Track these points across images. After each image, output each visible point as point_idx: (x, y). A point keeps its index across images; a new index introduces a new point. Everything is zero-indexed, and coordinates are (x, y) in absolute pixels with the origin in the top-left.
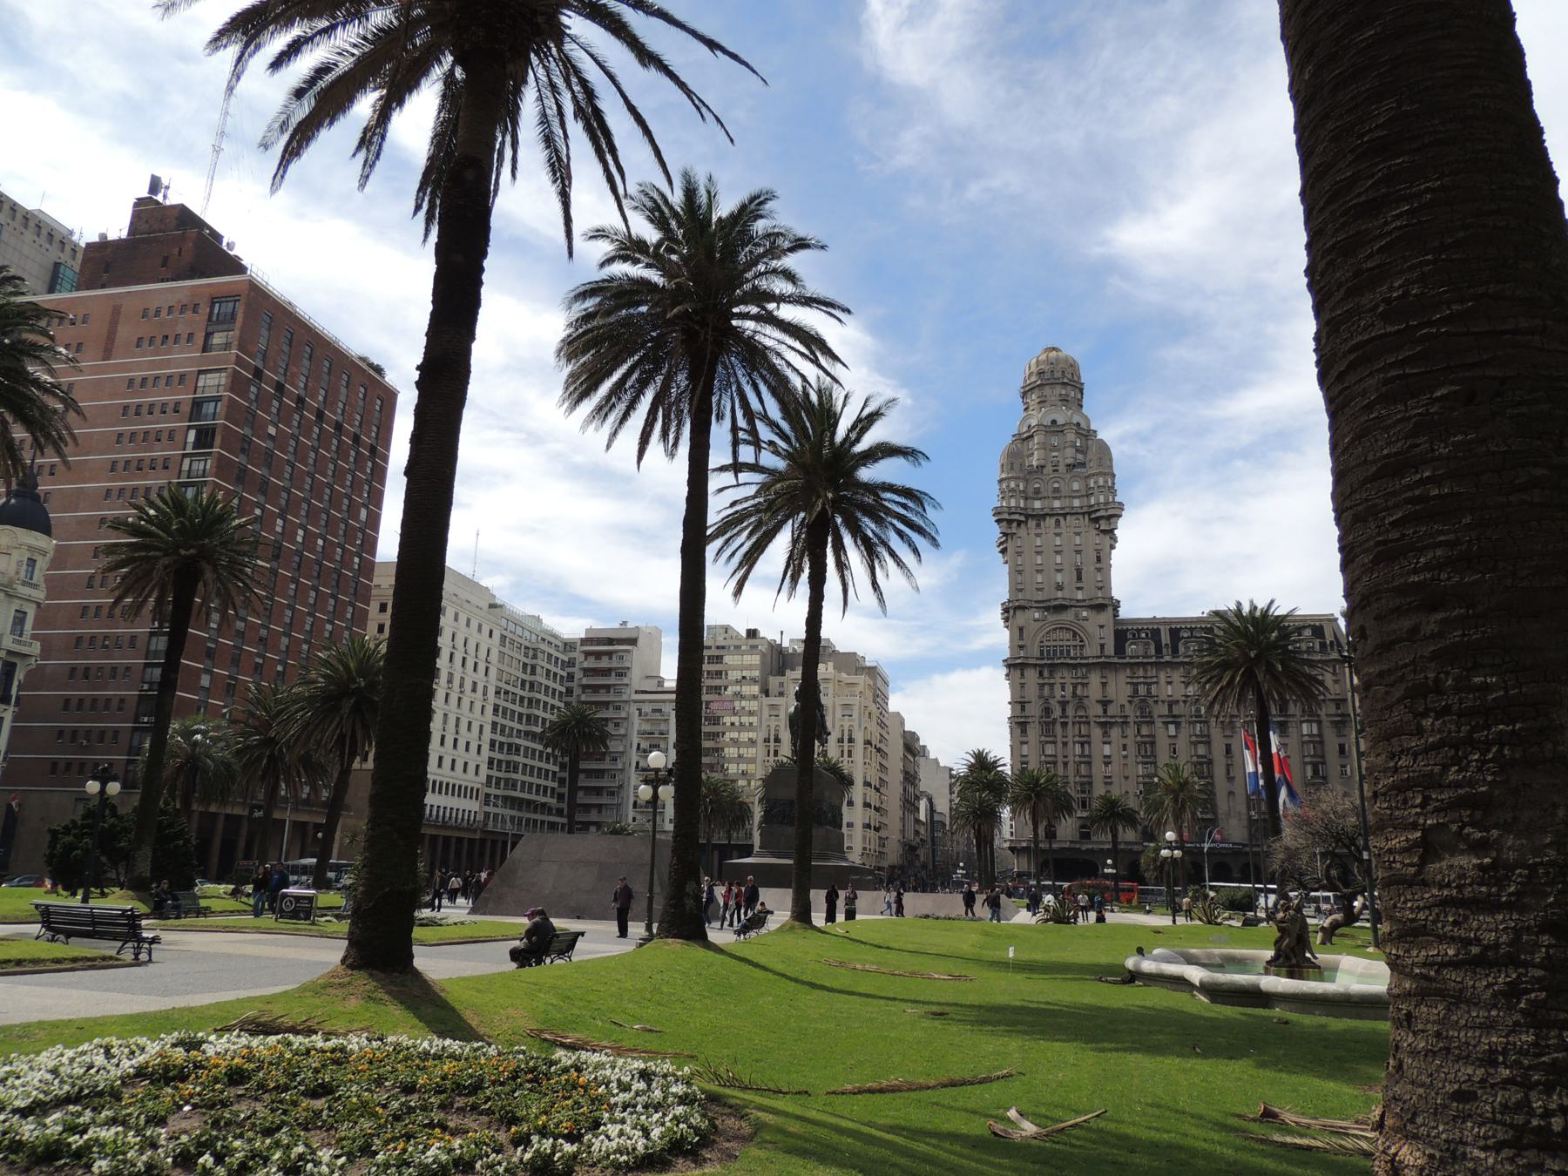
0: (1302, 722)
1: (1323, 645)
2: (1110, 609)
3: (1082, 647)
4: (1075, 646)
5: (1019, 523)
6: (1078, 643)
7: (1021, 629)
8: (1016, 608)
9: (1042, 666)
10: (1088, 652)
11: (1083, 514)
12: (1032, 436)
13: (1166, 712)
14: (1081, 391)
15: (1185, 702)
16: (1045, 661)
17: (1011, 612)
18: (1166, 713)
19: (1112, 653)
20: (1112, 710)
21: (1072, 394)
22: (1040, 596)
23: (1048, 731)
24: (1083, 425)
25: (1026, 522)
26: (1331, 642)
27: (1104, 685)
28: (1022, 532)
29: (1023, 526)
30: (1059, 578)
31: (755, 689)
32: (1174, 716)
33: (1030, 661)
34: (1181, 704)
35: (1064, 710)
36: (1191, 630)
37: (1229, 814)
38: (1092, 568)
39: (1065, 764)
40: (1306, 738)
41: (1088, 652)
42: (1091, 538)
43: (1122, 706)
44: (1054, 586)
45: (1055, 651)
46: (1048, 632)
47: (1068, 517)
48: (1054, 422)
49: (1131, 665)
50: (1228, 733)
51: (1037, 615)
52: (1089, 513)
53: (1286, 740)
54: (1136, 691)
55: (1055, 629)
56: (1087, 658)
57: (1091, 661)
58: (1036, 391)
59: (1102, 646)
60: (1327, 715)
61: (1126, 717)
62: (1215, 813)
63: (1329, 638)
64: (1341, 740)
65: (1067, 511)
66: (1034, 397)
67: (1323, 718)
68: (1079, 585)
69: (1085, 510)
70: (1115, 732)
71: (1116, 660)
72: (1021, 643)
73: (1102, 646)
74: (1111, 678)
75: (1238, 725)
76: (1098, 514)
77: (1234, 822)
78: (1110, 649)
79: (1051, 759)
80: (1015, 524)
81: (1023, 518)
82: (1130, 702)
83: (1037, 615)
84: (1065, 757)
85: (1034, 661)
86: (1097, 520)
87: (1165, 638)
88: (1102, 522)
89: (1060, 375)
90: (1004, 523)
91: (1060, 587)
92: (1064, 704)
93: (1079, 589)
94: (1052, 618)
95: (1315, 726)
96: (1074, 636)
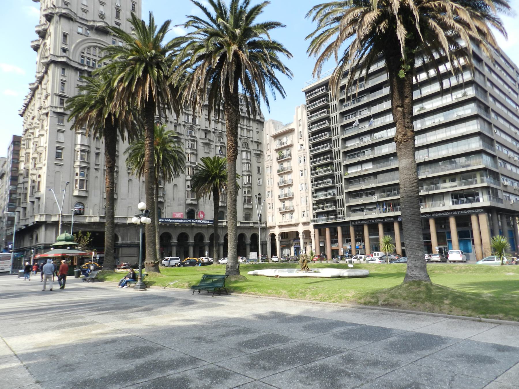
0: (242, 151)
7: (65, 36)
8: (62, 16)
9: (82, 72)
15: (184, 126)
16: (86, 68)
17: (56, 18)
22: (84, 16)
30: (101, 9)
32: (178, 133)
33: (73, 64)
34: (182, 126)
39: (97, 155)
40: (245, 161)
46: (89, 48)
50: (207, 151)
51: (80, 30)
55: (95, 47)
60: (254, 150)
64: (259, 165)
67: (252, 151)
75: (212, 147)
79: (86, 148)
83: (80, 30)
85: (76, 65)
94: (93, 36)
95: (249, 154)
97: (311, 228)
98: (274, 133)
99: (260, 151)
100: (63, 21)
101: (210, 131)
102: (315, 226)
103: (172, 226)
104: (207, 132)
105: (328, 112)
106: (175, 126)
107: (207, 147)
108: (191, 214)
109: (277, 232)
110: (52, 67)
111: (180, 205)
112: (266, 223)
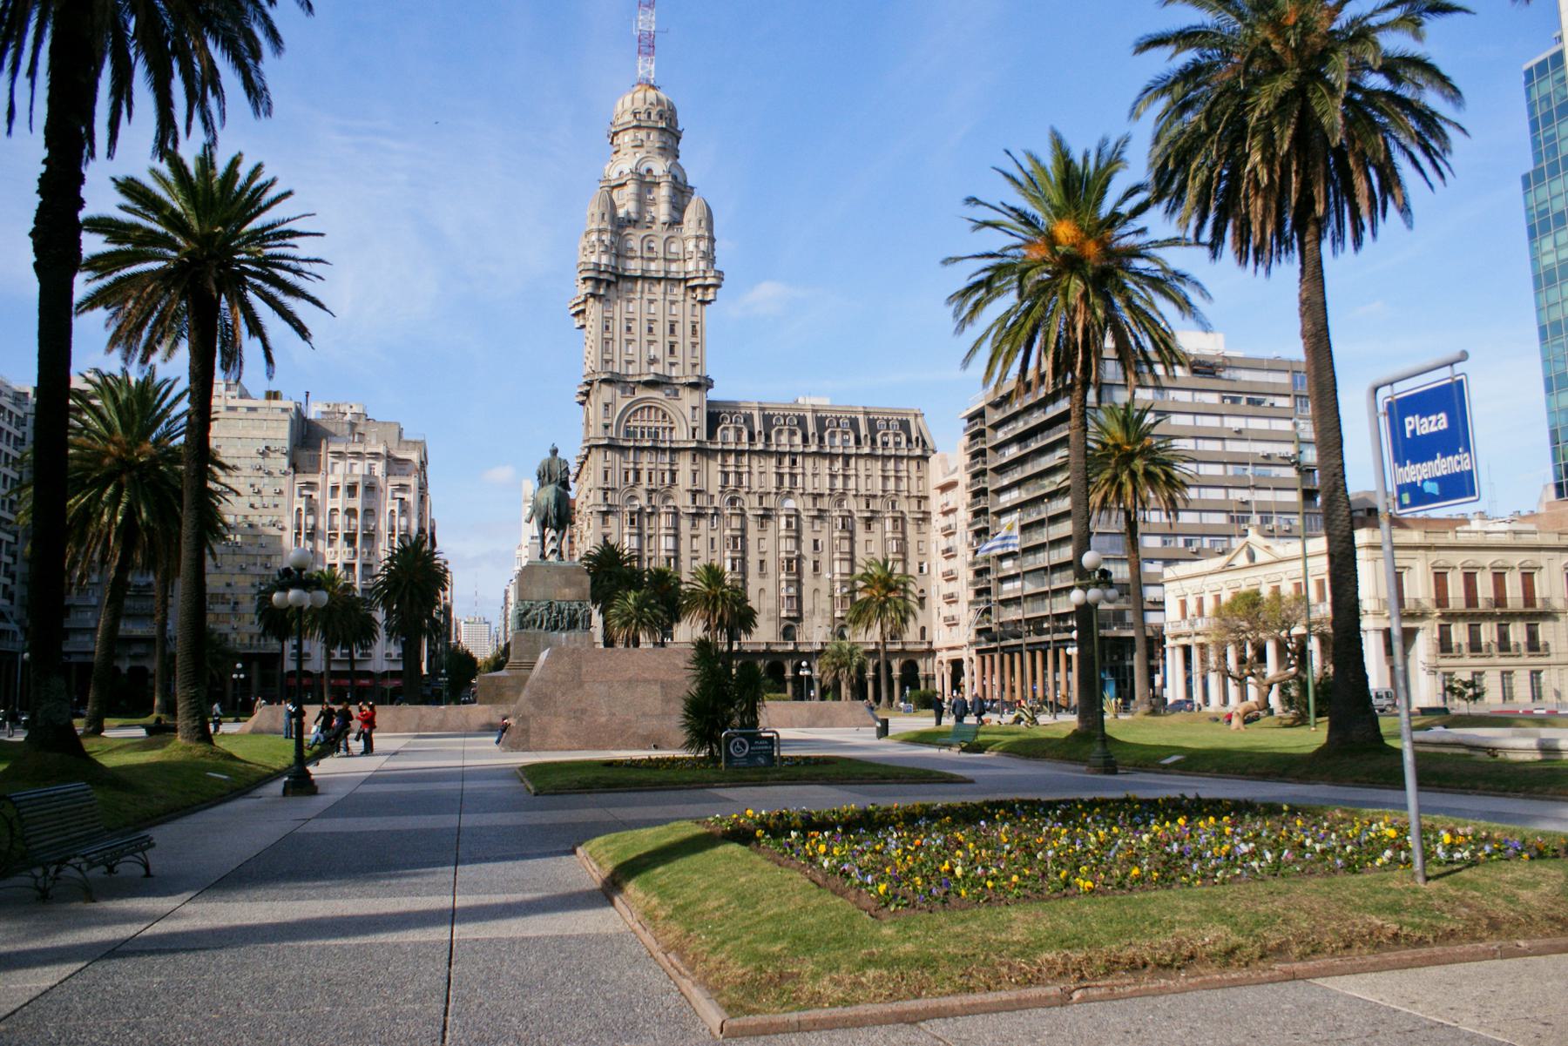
1: (909, 440)
2: (704, 388)
3: (672, 429)
4: (664, 429)
5: (609, 283)
6: (667, 424)
7: (606, 405)
8: (604, 381)
10: (676, 435)
11: (680, 280)
12: (625, 184)
13: (756, 504)
14: (678, 139)
15: (776, 494)
17: (596, 385)
18: (757, 505)
19: (705, 439)
20: (701, 500)
21: (670, 142)
23: (632, 522)
24: (680, 179)
25: (616, 283)
26: (917, 439)
27: (694, 473)
28: (612, 293)
29: (612, 287)
31: (284, 462)
34: (773, 497)
35: (650, 499)
36: (785, 417)
37: (813, 612)
38: (688, 343)
41: (676, 435)
42: (684, 309)
43: (712, 496)
44: (645, 359)
45: (643, 434)
47: (663, 283)
48: (649, 171)
49: (725, 453)
52: (686, 280)
53: (870, 536)
54: (726, 480)
56: (678, 442)
57: (682, 445)
58: (631, 132)
59: (694, 429)
61: (716, 508)
62: (800, 609)
63: (914, 435)
65: (662, 274)
66: (627, 139)
68: (673, 360)
69: (682, 276)
70: (703, 524)
71: (709, 446)
72: (607, 421)
73: (694, 429)
74: (702, 461)
76: (695, 282)
77: (817, 620)
78: (702, 434)
80: (604, 285)
81: (613, 279)
82: (721, 492)
84: (650, 551)
86: (694, 288)
87: (758, 426)
88: (699, 291)
89: (657, 118)
90: (589, 283)
91: (652, 361)
92: (650, 492)
93: (672, 364)
96: (664, 416)
97: (973, 651)
98: (943, 481)
99: (924, 512)
100: (605, 388)
101: (821, 495)
102: (978, 652)
103: (756, 654)
104: (816, 496)
105: (985, 463)
106: (761, 498)
107: (817, 522)
108: (788, 633)
109: (944, 656)
110: (593, 450)
111: (769, 619)
112: (930, 643)
